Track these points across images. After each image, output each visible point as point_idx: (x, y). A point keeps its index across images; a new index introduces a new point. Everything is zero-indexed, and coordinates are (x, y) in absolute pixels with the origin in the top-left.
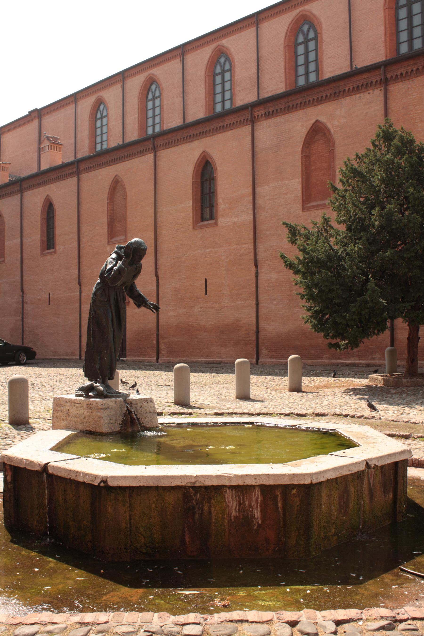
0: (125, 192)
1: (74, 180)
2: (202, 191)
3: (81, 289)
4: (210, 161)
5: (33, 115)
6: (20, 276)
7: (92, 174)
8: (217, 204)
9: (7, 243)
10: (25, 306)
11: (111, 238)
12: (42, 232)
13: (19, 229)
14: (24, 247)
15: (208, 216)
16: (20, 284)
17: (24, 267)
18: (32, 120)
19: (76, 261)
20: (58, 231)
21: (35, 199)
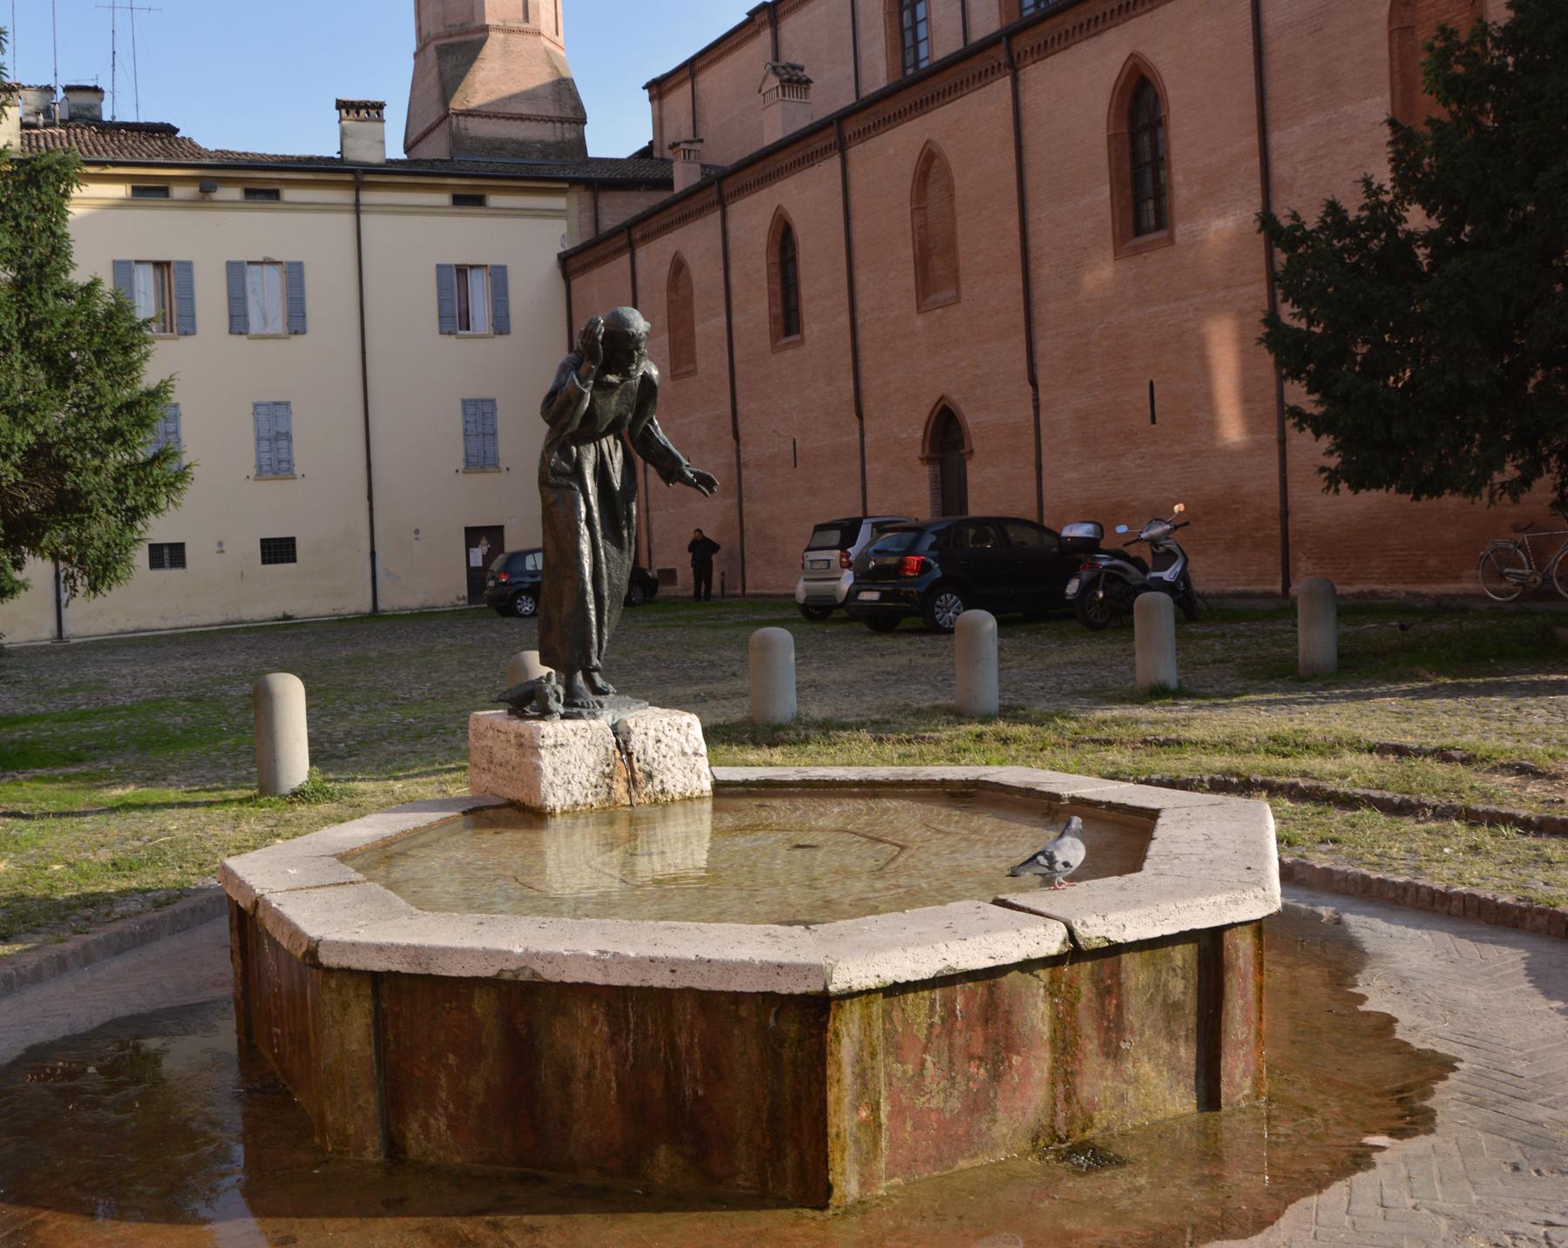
0: (951, 179)
1: (835, 162)
2: (1135, 156)
3: (861, 424)
4: (1149, 75)
5: (759, 19)
6: (729, 403)
7: (873, 143)
8: (1171, 188)
9: (698, 329)
10: (744, 473)
11: (926, 296)
12: (771, 294)
13: (723, 292)
14: (735, 333)
15: (1153, 222)
16: (730, 421)
17: (738, 383)
18: (757, 33)
19: (849, 359)
20: (806, 290)
21: (751, 218)
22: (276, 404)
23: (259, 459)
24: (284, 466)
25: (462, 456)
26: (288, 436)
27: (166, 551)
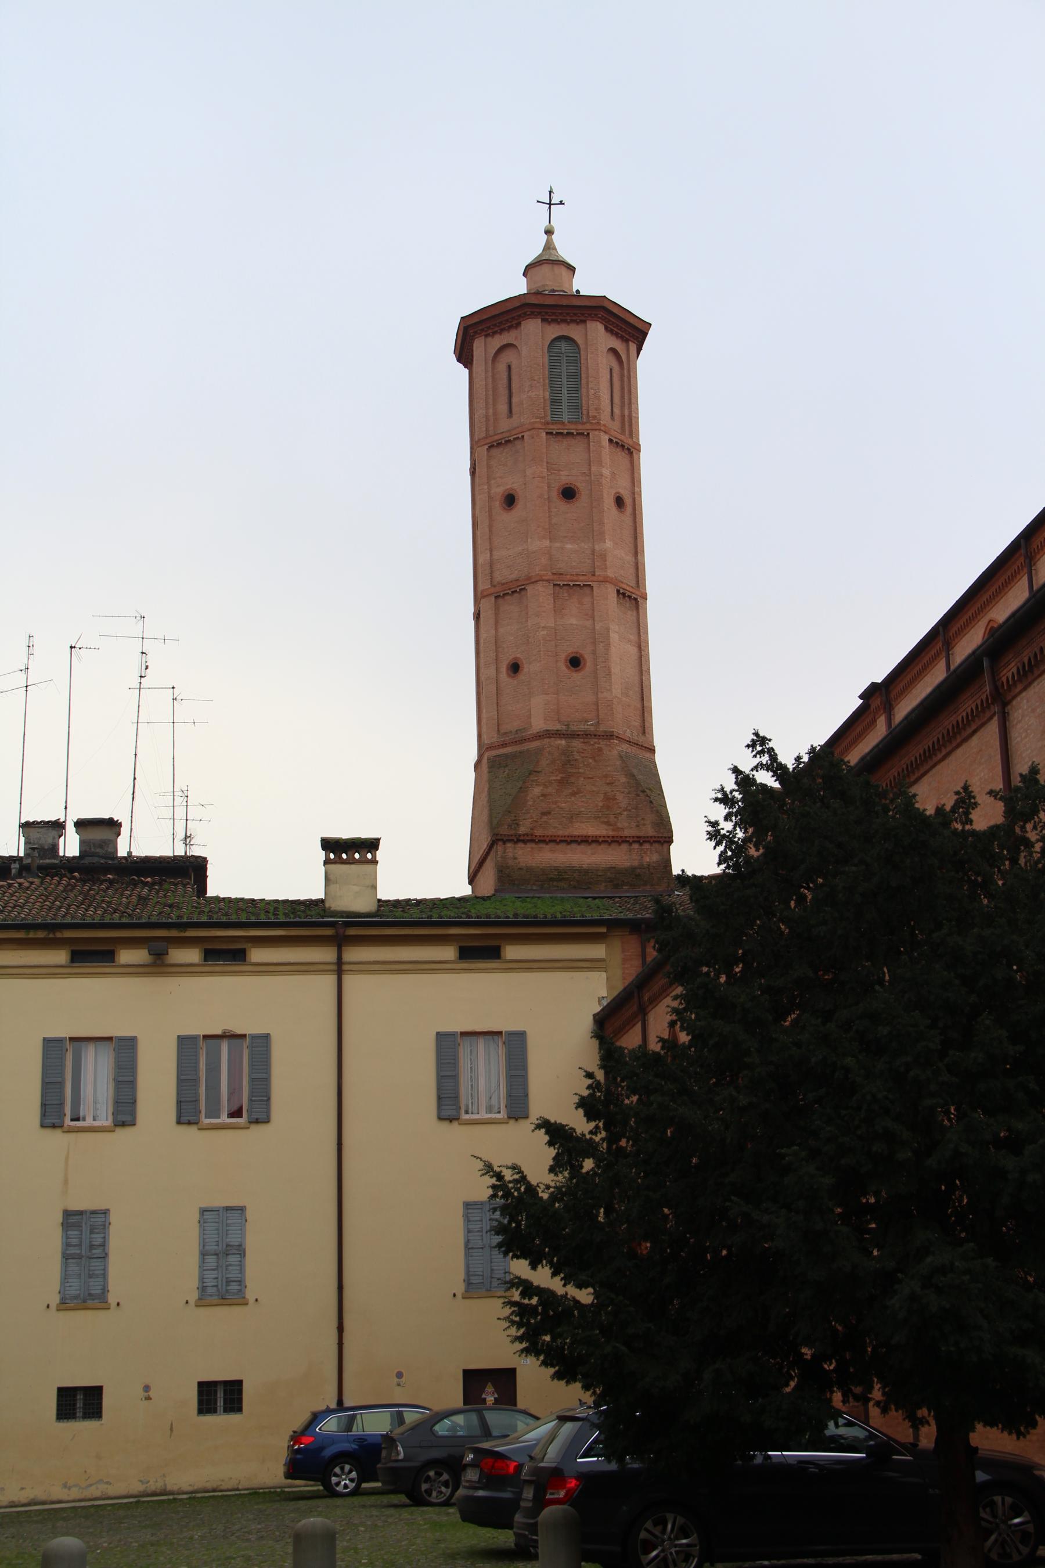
22: (228, 1209)
23: (202, 1279)
24: (234, 1287)
25: (461, 1275)
26: (240, 1250)
27: (80, 1397)
